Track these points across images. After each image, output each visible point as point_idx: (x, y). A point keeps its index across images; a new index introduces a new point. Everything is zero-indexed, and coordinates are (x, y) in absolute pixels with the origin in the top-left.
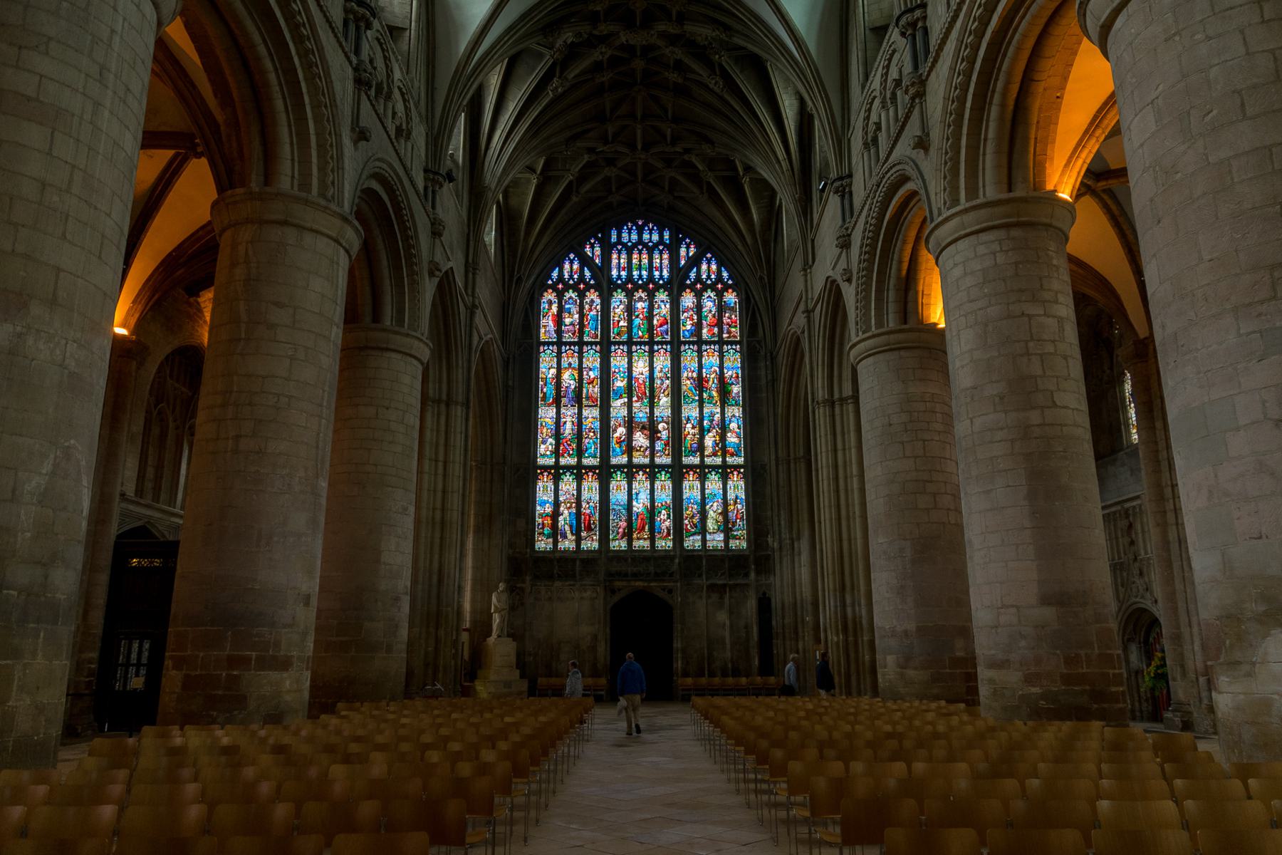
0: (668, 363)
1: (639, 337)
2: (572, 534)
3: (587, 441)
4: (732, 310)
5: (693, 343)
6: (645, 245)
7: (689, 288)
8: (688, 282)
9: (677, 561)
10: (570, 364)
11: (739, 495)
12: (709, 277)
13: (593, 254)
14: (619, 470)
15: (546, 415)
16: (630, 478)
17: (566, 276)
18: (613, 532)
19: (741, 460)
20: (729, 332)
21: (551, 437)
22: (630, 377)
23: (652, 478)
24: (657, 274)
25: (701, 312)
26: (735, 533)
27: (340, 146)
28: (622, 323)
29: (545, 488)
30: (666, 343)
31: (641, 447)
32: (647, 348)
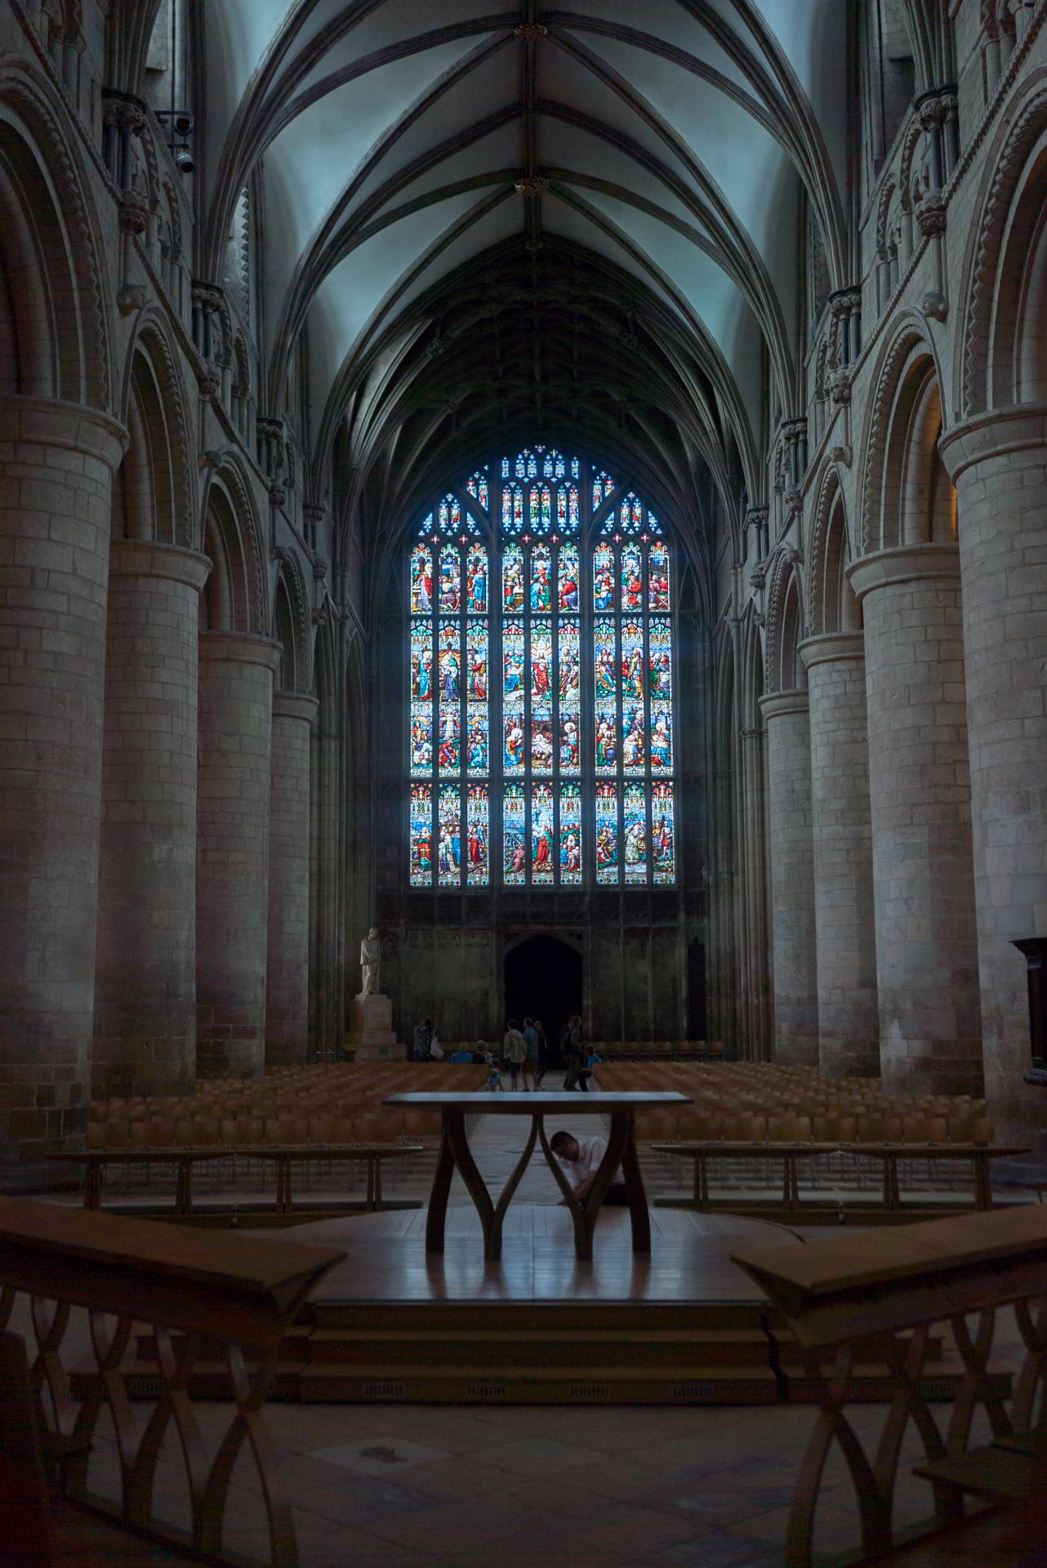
0: (576, 644)
1: (539, 609)
2: (456, 866)
3: (473, 746)
4: (662, 570)
5: (609, 616)
6: (547, 482)
7: (604, 541)
8: (604, 532)
10: (450, 645)
11: (666, 815)
12: (631, 525)
13: (478, 494)
14: (514, 783)
15: (420, 712)
16: (529, 795)
17: (443, 525)
18: (507, 862)
19: (669, 771)
20: (657, 601)
21: (427, 741)
22: (528, 663)
23: (557, 795)
24: (562, 521)
25: (621, 573)
26: (661, 864)
27: (264, 568)
28: (517, 590)
29: (421, 808)
30: (575, 616)
31: (542, 754)
32: (549, 623)
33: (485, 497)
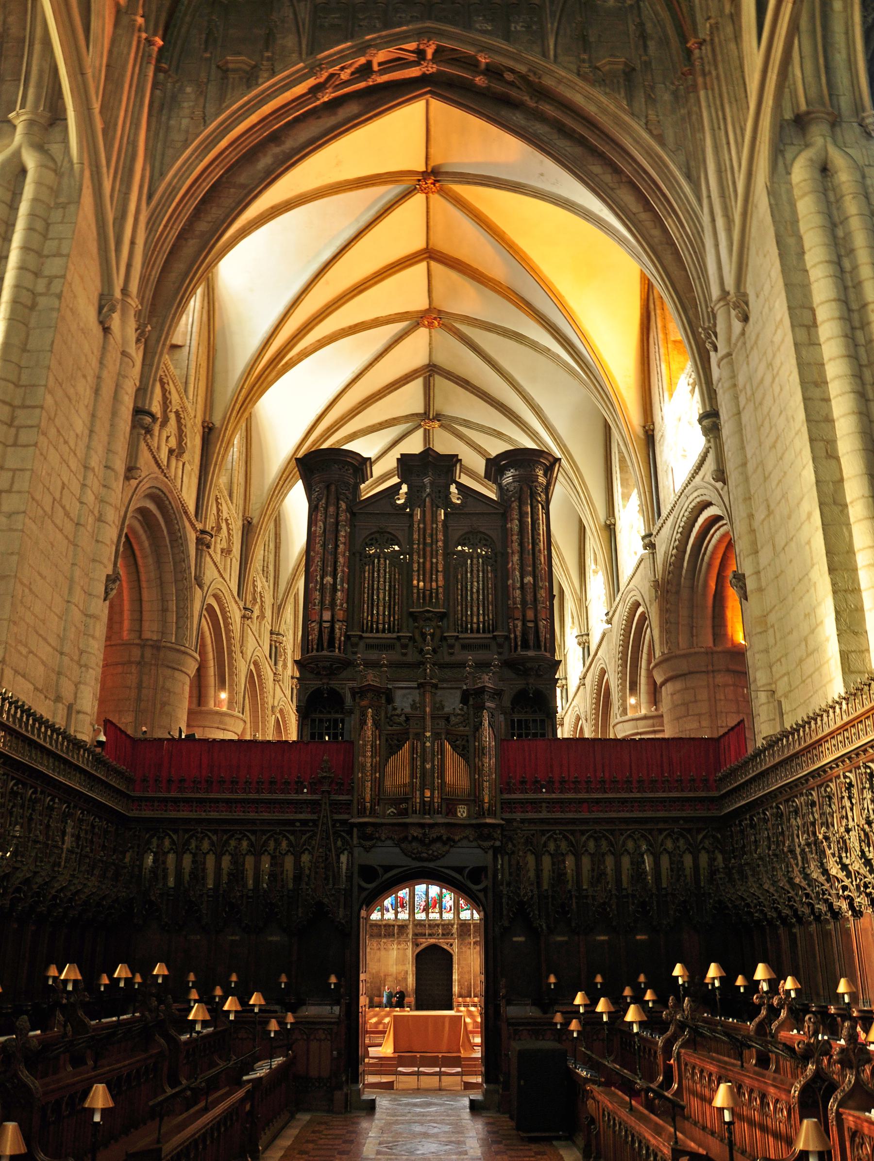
9: (455, 926)
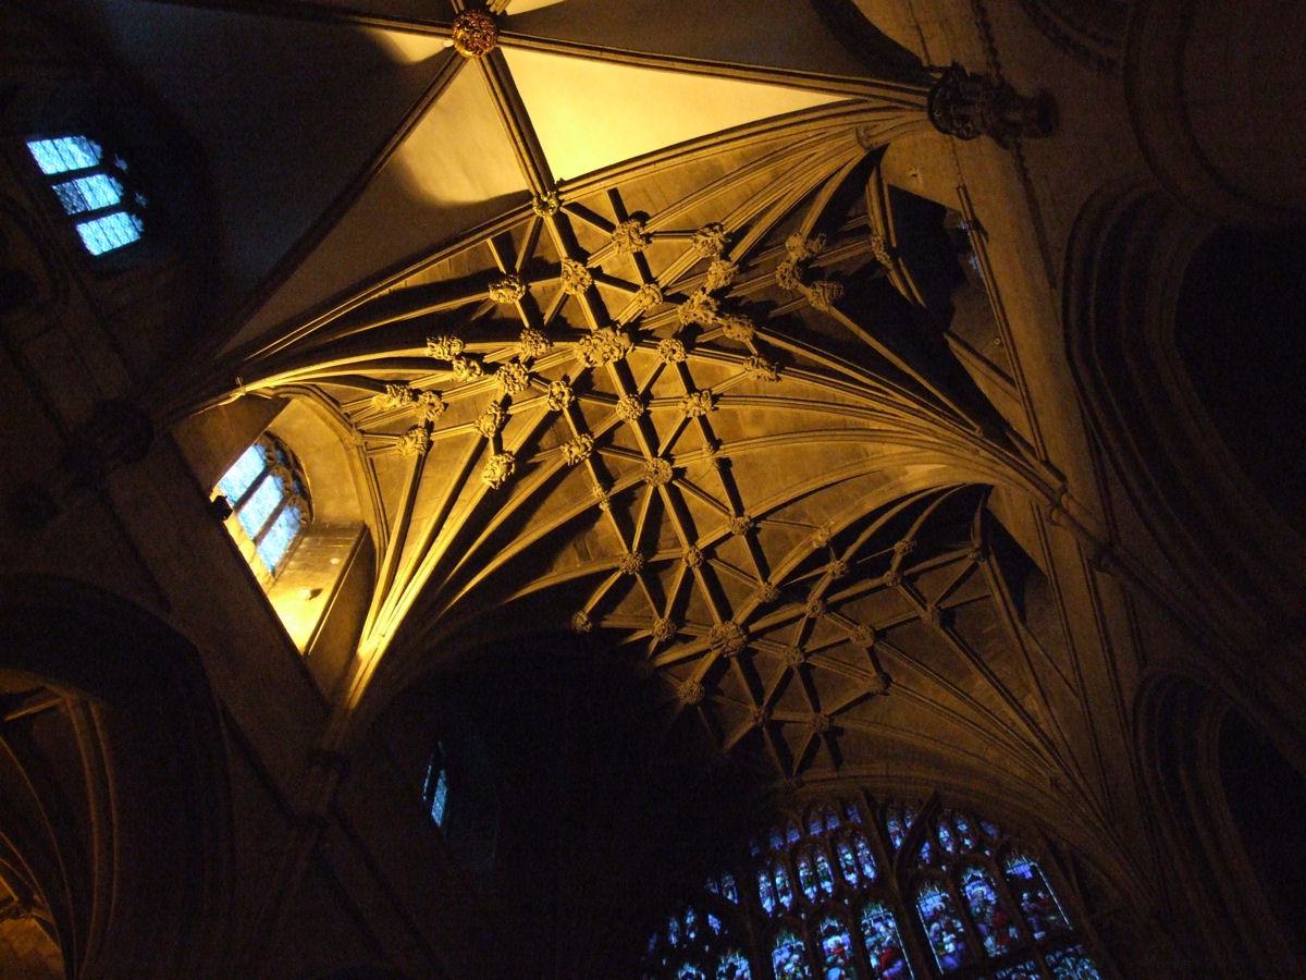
33: (731, 888)
